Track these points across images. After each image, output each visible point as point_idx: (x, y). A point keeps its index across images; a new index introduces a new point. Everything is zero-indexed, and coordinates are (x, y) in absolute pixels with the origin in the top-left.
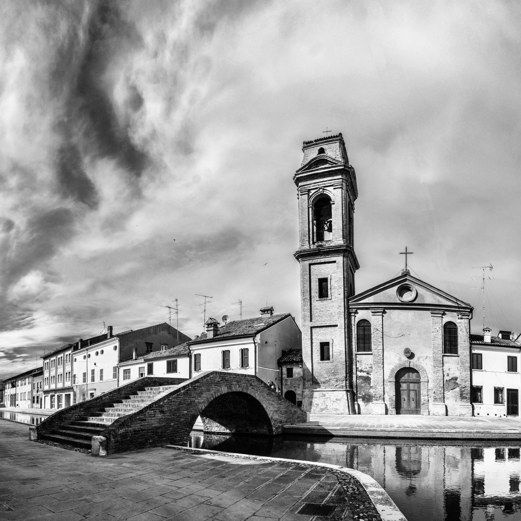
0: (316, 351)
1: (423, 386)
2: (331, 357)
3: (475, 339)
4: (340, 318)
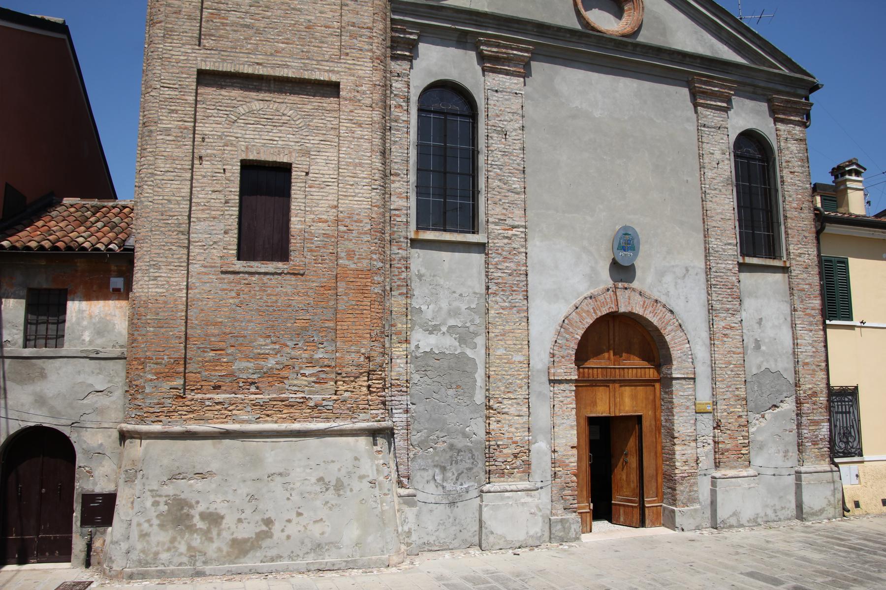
0: (217, 200)
1: (680, 392)
2: (295, 243)
3: (829, 215)
4: (355, 53)
